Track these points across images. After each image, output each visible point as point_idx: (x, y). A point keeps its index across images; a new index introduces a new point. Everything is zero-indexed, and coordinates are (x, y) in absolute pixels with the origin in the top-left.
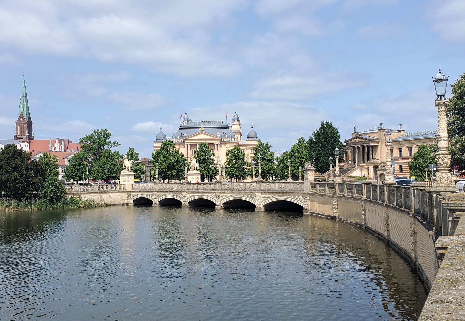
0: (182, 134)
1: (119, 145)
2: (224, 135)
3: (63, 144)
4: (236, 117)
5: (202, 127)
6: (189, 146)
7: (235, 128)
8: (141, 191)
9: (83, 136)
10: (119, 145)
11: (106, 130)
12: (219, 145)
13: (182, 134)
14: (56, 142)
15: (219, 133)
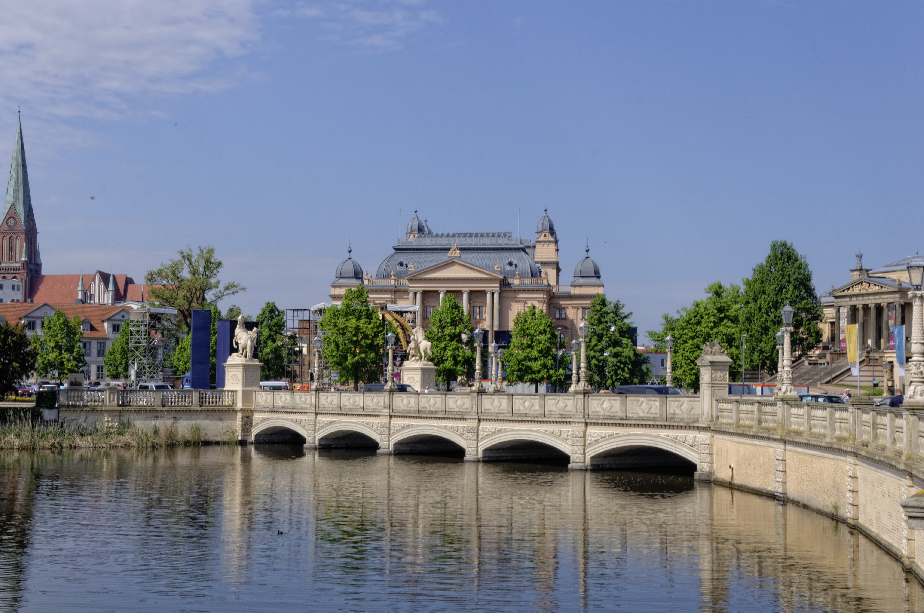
0: (401, 264)
1: (243, 289)
2: (513, 268)
4: (547, 224)
5: (454, 247)
6: (418, 296)
7: (545, 252)
9: (156, 268)
10: (243, 289)
12: (496, 296)
13: (401, 264)
14: (94, 280)
15: (498, 264)
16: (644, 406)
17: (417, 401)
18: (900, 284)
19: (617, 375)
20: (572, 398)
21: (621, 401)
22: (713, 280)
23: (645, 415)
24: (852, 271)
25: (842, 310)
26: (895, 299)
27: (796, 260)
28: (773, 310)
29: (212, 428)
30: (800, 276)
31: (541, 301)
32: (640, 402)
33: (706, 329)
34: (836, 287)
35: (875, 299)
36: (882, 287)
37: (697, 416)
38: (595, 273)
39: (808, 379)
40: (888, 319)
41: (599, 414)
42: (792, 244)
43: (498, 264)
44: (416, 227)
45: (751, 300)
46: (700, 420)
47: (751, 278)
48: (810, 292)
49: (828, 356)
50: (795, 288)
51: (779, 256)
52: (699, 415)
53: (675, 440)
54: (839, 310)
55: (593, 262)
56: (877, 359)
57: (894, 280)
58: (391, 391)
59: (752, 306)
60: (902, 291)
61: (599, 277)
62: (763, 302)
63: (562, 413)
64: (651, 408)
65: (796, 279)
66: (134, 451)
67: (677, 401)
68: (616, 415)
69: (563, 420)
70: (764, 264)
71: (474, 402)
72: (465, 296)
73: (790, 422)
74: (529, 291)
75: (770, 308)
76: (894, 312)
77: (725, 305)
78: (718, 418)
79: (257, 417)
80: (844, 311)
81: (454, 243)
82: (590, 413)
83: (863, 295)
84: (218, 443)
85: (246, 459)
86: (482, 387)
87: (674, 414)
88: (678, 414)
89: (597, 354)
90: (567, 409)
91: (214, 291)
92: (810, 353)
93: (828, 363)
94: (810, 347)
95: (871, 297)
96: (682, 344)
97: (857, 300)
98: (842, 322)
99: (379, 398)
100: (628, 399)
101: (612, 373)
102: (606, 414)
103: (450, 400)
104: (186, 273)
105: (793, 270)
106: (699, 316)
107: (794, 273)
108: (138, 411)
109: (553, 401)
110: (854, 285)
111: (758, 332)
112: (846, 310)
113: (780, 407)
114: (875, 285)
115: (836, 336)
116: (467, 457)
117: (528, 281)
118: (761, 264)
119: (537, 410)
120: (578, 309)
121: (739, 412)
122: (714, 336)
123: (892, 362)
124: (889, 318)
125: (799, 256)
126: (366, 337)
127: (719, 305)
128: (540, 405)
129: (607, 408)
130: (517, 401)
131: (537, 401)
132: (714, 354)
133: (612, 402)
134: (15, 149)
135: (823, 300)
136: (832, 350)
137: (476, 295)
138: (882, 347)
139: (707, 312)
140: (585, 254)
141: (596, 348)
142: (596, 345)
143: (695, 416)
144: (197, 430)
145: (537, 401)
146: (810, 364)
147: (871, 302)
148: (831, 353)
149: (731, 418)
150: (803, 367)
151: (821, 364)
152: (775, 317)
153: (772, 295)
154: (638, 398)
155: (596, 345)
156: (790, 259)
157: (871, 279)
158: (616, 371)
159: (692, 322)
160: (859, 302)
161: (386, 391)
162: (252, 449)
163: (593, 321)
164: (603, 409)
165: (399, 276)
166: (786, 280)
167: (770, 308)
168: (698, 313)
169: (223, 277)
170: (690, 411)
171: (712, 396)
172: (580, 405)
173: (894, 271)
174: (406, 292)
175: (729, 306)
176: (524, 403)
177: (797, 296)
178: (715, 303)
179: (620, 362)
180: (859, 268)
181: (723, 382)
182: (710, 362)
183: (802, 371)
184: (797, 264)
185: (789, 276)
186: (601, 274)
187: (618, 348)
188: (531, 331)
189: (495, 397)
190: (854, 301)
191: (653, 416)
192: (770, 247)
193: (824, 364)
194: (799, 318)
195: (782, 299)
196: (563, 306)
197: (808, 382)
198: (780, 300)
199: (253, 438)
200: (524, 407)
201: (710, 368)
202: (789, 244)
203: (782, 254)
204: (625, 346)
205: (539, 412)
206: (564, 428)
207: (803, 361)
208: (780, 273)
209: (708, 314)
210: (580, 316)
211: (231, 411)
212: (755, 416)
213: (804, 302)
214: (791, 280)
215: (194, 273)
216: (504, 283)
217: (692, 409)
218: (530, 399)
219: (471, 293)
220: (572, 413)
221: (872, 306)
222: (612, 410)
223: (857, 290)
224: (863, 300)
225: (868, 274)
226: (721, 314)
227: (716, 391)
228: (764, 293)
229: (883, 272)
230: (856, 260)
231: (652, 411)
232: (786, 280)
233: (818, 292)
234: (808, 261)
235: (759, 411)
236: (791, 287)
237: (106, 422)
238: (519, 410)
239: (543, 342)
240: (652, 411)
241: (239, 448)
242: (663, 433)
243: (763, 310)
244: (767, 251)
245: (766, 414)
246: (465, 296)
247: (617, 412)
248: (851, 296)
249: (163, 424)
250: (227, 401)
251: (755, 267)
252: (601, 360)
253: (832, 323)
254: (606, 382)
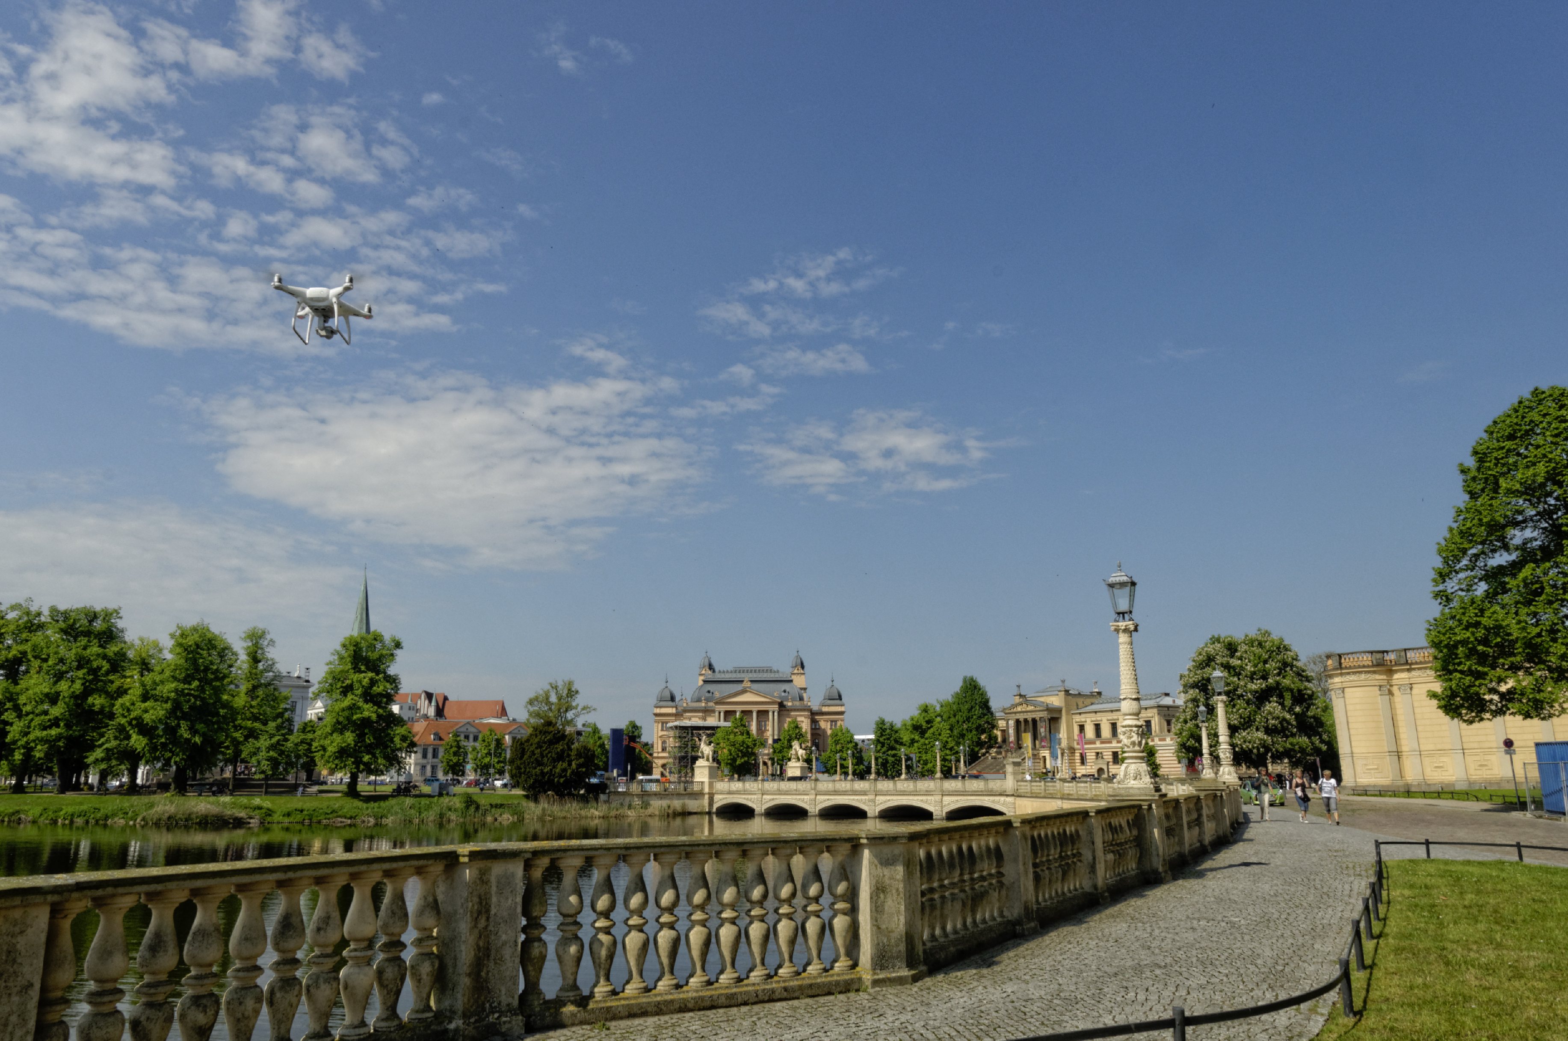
3: (433, 703)
5: (746, 679)
7: (799, 681)
8: (730, 793)
9: (532, 695)
11: (570, 683)
15: (777, 691)
26: (1044, 714)
29: (692, 805)
43: (777, 691)
44: (707, 664)
48: (988, 708)
53: (993, 801)
58: (763, 780)
59: (953, 720)
60: (1049, 709)
66: (657, 818)
69: (928, 793)
72: (755, 715)
74: (798, 710)
79: (717, 797)
80: (1012, 723)
81: (746, 677)
84: (695, 813)
85: (711, 822)
91: (574, 711)
94: (991, 747)
104: (553, 699)
108: (656, 794)
110: (1016, 705)
116: (869, 815)
117: (798, 703)
126: (748, 747)
134: (362, 595)
135: (997, 714)
137: (762, 714)
144: (684, 805)
147: (1029, 717)
160: (1021, 717)
162: (714, 817)
165: (707, 700)
166: (973, 703)
169: (579, 701)
174: (713, 711)
190: (1018, 716)
199: (714, 810)
206: (929, 798)
211: (701, 794)
215: (560, 698)
216: (781, 705)
219: (759, 712)
223: (1019, 709)
232: (973, 703)
233: (993, 709)
237: (637, 802)
241: (707, 817)
242: (986, 798)
246: (755, 715)
249: (664, 803)
250: (696, 788)
253: (1003, 731)
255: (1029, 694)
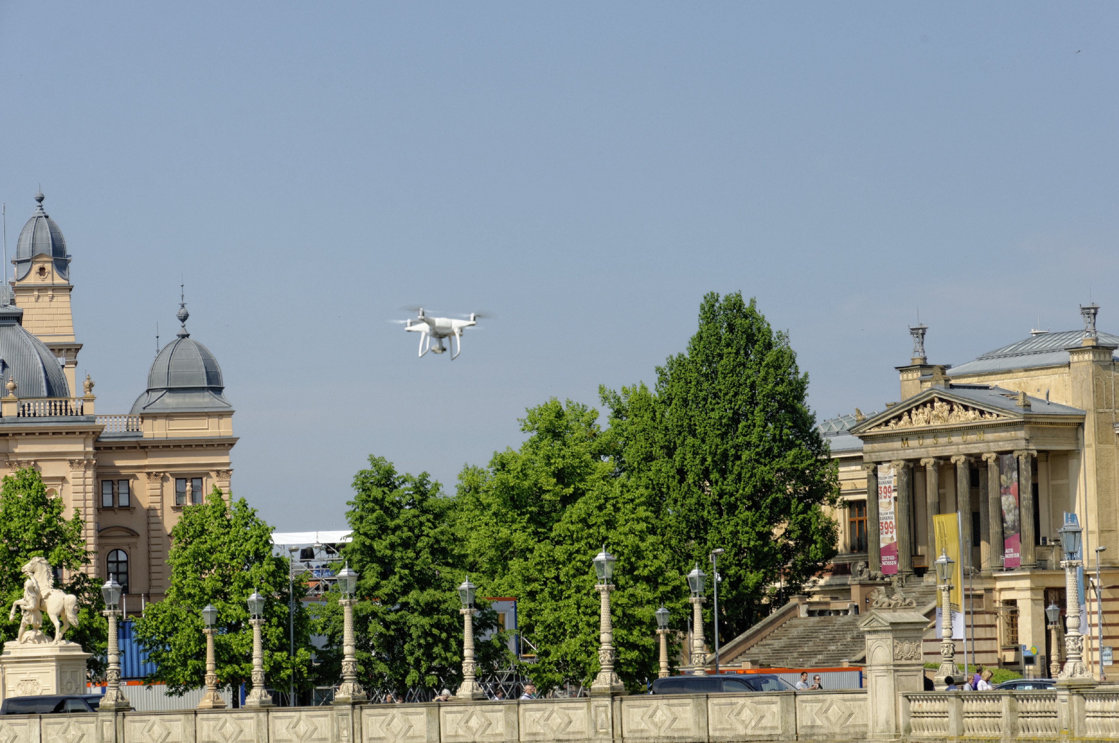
16: (746, 714)
17: (190, 730)
18: (1027, 406)
19: (430, 657)
20: (585, 705)
21: (697, 706)
22: (539, 397)
23: (749, 732)
24: (902, 370)
25: (883, 471)
26: (1015, 441)
27: (769, 346)
28: (714, 476)
30: (780, 389)
31: (80, 463)
32: (739, 706)
33: (631, 537)
34: (866, 415)
35: (965, 443)
36: (982, 413)
37: (863, 729)
38: (209, 381)
39: (815, 653)
40: (1001, 494)
41: (645, 735)
42: (753, 302)
45: (656, 451)
46: (870, 734)
47: (653, 393)
48: (802, 423)
49: (856, 592)
50: (771, 418)
51: (723, 331)
52: (866, 726)
54: (875, 471)
55: (201, 349)
56: (980, 596)
57: (1012, 395)
61: (218, 390)
62: (689, 456)
63: (561, 737)
64: (762, 717)
65: (771, 396)
67: (818, 701)
68: (686, 734)
70: (687, 356)
71: (343, 725)
73: (1085, 726)
75: (706, 474)
76: (1015, 475)
77: (576, 462)
78: (908, 730)
80: (889, 476)
82: (626, 734)
83: (935, 433)
86: (123, 698)
87: (812, 727)
88: (821, 727)
89: (378, 606)
90: (571, 729)
92: (807, 587)
93: (857, 607)
94: (810, 570)
95: (955, 439)
96: (574, 576)
97: (921, 446)
98: (883, 501)
99: (84, 726)
100: (710, 701)
101: (418, 653)
102: (662, 734)
103: (278, 722)
105: (762, 373)
106: (609, 506)
107: (765, 379)
109: (538, 714)
111: (680, 533)
112: (893, 472)
113: (1063, 701)
114: (966, 408)
115: (871, 538)
118: (681, 356)
119: (501, 735)
120: (164, 479)
121: (962, 715)
122: (651, 556)
123: (1012, 603)
124: (1004, 490)
125: (775, 335)
127: (560, 463)
128: (507, 723)
129: (663, 722)
130: (449, 716)
131: (500, 715)
132: (895, 608)
133: (673, 709)
136: (865, 576)
138: (985, 565)
139: (628, 496)
140: (177, 328)
141: (376, 593)
142: (377, 586)
143: (857, 729)
145: (500, 715)
146: (811, 613)
147: (957, 449)
148: (862, 585)
149: (945, 727)
150: (795, 622)
151: (837, 612)
152: (721, 496)
153: (713, 439)
154: (734, 700)
155: (377, 586)
156: (755, 343)
157: (956, 391)
158: (428, 648)
159: (592, 520)
160: (926, 451)
161: (106, 710)
163: (365, 527)
164: (655, 725)
167: (706, 474)
168: (607, 499)
170: (847, 720)
171: (896, 688)
172: (604, 717)
173: (1009, 371)
175: (587, 466)
176: (467, 722)
177: (774, 440)
178: (548, 458)
179: (438, 625)
180: (918, 362)
181: (914, 661)
182: (892, 624)
183: (794, 632)
184: (770, 357)
185: (753, 386)
186: (226, 381)
187: (431, 591)
188: (223, 557)
189: (471, 709)
190: (915, 449)
191: (767, 732)
192: (698, 311)
193: (846, 612)
194: (780, 495)
195: (737, 447)
196: (124, 472)
197: (814, 660)
198: (733, 451)
200: (469, 728)
201: (890, 635)
202: (747, 304)
203: (731, 328)
204: (445, 585)
205: (509, 738)
207: (795, 607)
208: (729, 379)
209: (632, 500)
210: (170, 501)
212: (1004, 721)
213: (791, 454)
214: (759, 398)
217: (850, 715)
218: (482, 711)
220: (585, 736)
221: (960, 460)
222: (675, 725)
223: (919, 420)
224: (936, 445)
225: (947, 380)
226: (567, 486)
227: (903, 678)
228: (693, 433)
229: (979, 375)
230: (912, 341)
231: (765, 722)
233: (820, 426)
234: (794, 346)
235: (1012, 710)
236: (759, 418)
238: (456, 736)
239: (256, 583)
240: (765, 722)
243: (690, 479)
244: (691, 325)
245: (1026, 714)
247: (686, 730)
248: (904, 437)
251: (663, 364)
252: (394, 623)
253: (856, 507)
254: (404, 676)
255: (962, 366)
